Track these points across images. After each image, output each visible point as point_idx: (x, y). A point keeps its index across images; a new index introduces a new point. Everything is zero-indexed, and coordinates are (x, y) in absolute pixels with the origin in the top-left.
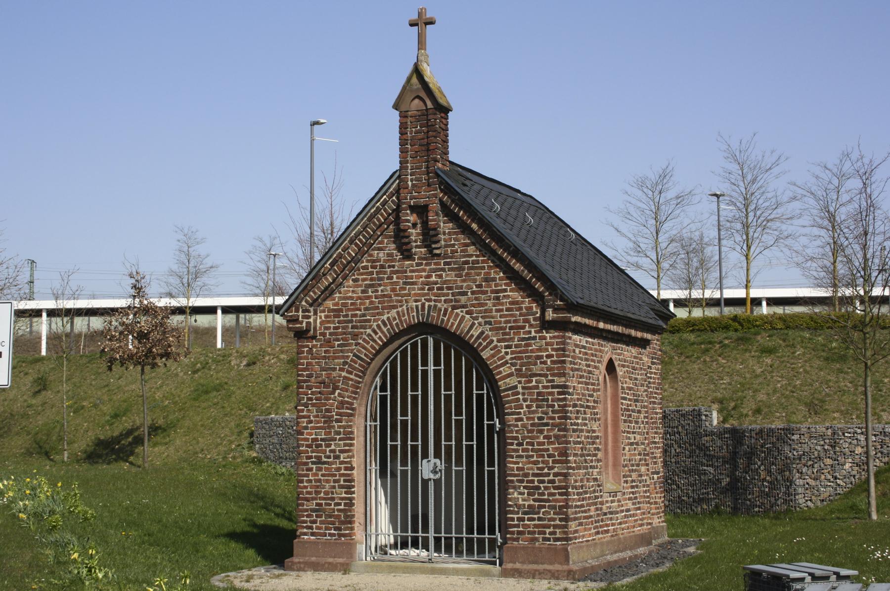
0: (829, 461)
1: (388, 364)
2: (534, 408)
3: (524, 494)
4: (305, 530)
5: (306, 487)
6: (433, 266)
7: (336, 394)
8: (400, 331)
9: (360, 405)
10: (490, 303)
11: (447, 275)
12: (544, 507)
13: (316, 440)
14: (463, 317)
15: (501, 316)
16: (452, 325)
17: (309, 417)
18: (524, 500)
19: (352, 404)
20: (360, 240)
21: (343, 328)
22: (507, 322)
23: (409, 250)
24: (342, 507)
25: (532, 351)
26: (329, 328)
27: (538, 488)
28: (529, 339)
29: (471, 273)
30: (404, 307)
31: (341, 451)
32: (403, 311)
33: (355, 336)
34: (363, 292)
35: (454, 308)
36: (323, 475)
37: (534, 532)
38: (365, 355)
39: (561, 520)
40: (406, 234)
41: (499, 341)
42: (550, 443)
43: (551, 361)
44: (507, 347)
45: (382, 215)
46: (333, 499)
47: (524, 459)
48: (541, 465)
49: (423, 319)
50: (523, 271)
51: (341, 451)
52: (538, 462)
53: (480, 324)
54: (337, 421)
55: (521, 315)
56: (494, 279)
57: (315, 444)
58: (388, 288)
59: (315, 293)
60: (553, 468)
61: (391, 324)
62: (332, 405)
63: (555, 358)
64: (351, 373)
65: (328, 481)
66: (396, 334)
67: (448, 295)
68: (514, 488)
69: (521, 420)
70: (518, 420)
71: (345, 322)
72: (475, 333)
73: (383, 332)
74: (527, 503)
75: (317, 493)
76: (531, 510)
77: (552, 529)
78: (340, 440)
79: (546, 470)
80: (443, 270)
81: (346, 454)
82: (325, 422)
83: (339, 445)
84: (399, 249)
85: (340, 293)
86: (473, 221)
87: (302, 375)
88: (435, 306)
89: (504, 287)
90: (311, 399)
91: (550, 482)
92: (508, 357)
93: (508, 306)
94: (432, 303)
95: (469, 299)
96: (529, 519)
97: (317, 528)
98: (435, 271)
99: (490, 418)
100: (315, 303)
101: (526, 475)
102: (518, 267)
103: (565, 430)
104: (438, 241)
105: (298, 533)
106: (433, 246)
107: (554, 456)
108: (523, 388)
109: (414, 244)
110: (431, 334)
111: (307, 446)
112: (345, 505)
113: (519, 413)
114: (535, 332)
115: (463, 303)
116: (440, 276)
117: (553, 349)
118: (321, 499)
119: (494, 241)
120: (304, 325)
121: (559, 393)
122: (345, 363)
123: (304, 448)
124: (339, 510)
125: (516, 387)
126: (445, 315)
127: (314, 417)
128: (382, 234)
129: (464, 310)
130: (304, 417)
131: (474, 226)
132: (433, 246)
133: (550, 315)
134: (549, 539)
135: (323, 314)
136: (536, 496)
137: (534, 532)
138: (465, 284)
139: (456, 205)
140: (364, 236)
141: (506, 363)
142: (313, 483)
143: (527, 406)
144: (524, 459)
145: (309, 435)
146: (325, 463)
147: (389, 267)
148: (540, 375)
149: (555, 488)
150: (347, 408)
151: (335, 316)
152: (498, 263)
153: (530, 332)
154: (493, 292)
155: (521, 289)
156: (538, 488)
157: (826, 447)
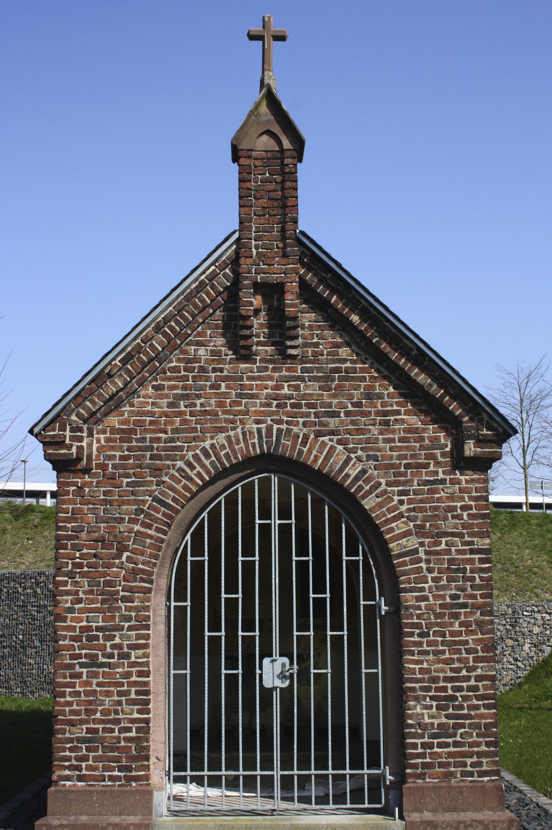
0: (510, 642)
1: (205, 514)
2: (444, 582)
3: (431, 707)
4: (67, 772)
5: (70, 704)
6: (284, 373)
7: (124, 558)
8: (232, 466)
9: (159, 575)
10: (375, 430)
11: (307, 387)
12: (463, 726)
13: (89, 629)
14: (332, 448)
15: (391, 449)
16: (315, 456)
17: (77, 593)
18: (431, 717)
19: (152, 573)
20: (172, 329)
21: (136, 458)
22: (399, 457)
23: (249, 347)
24: (133, 734)
25: (439, 500)
26: (113, 457)
27: (453, 698)
28: (435, 482)
29: (345, 386)
30: (239, 430)
31: (132, 647)
32: (236, 436)
33: (157, 471)
34: (170, 405)
35: (318, 434)
36: (98, 685)
37: (448, 764)
38: (174, 499)
39: (488, 744)
40: (248, 323)
41: (388, 484)
42: (468, 633)
43: (469, 515)
44: (401, 493)
45: (208, 294)
46: (117, 722)
47: (431, 657)
48: (456, 665)
49: (269, 449)
50: (430, 385)
51: (132, 647)
52: (453, 659)
53: (359, 459)
54: (124, 599)
55: (422, 448)
56: (380, 396)
57: (87, 635)
58: (212, 401)
59: (93, 403)
60: (474, 669)
61: (217, 455)
62: (117, 575)
63: (474, 511)
64: (149, 527)
65: (108, 694)
66: (225, 469)
67: (308, 415)
68: (417, 699)
69: (426, 599)
70: (418, 599)
71: (140, 449)
72: (353, 471)
73: (203, 466)
74: (436, 722)
75: (89, 712)
76: (444, 731)
77: (475, 759)
78: (130, 629)
79: (464, 672)
80: (302, 379)
81: (140, 652)
82: (103, 602)
83: (129, 638)
84: (232, 345)
85: (132, 405)
86: (352, 310)
87: (65, 529)
88: (289, 431)
89: (395, 408)
90: (80, 566)
91: (470, 689)
92: (404, 508)
93: (402, 434)
94: (284, 427)
95: (342, 422)
96: (440, 745)
97: (89, 768)
98: (288, 379)
99: (370, 595)
100: (92, 419)
101: (435, 680)
102: (422, 379)
103: (491, 613)
104: (296, 337)
105: (54, 777)
106: (288, 343)
107: (477, 652)
108: (427, 553)
109: (256, 340)
110: (275, 472)
111: (72, 638)
112: (138, 730)
113: (422, 589)
114: (444, 473)
115: (332, 427)
116: (297, 388)
117: (470, 498)
118: (95, 721)
119: (385, 340)
120: (74, 450)
121: (481, 561)
122: (140, 511)
123: (67, 642)
124: (126, 739)
125: (416, 551)
126: (304, 443)
127: (85, 593)
128: (203, 322)
129: (335, 438)
130: (68, 593)
131: (355, 318)
132: (288, 343)
133: (470, 449)
134: (471, 774)
135: (102, 436)
136: (451, 710)
137: (448, 764)
138: (335, 401)
139: (327, 286)
140: (178, 323)
141: (401, 515)
142: (83, 697)
143: (434, 579)
144: (431, 657)
145: (76, 621)
146: (103, 665)
147: (214, 370)
148: (453, 535)
149: (478, 698)
150: (142, 580)
151: (122, 440)
152: (386, 373)
153: (436, 473)
154: (378, 413)
155: (421, 411)
156: (453, 698)
157: (508, 627)
